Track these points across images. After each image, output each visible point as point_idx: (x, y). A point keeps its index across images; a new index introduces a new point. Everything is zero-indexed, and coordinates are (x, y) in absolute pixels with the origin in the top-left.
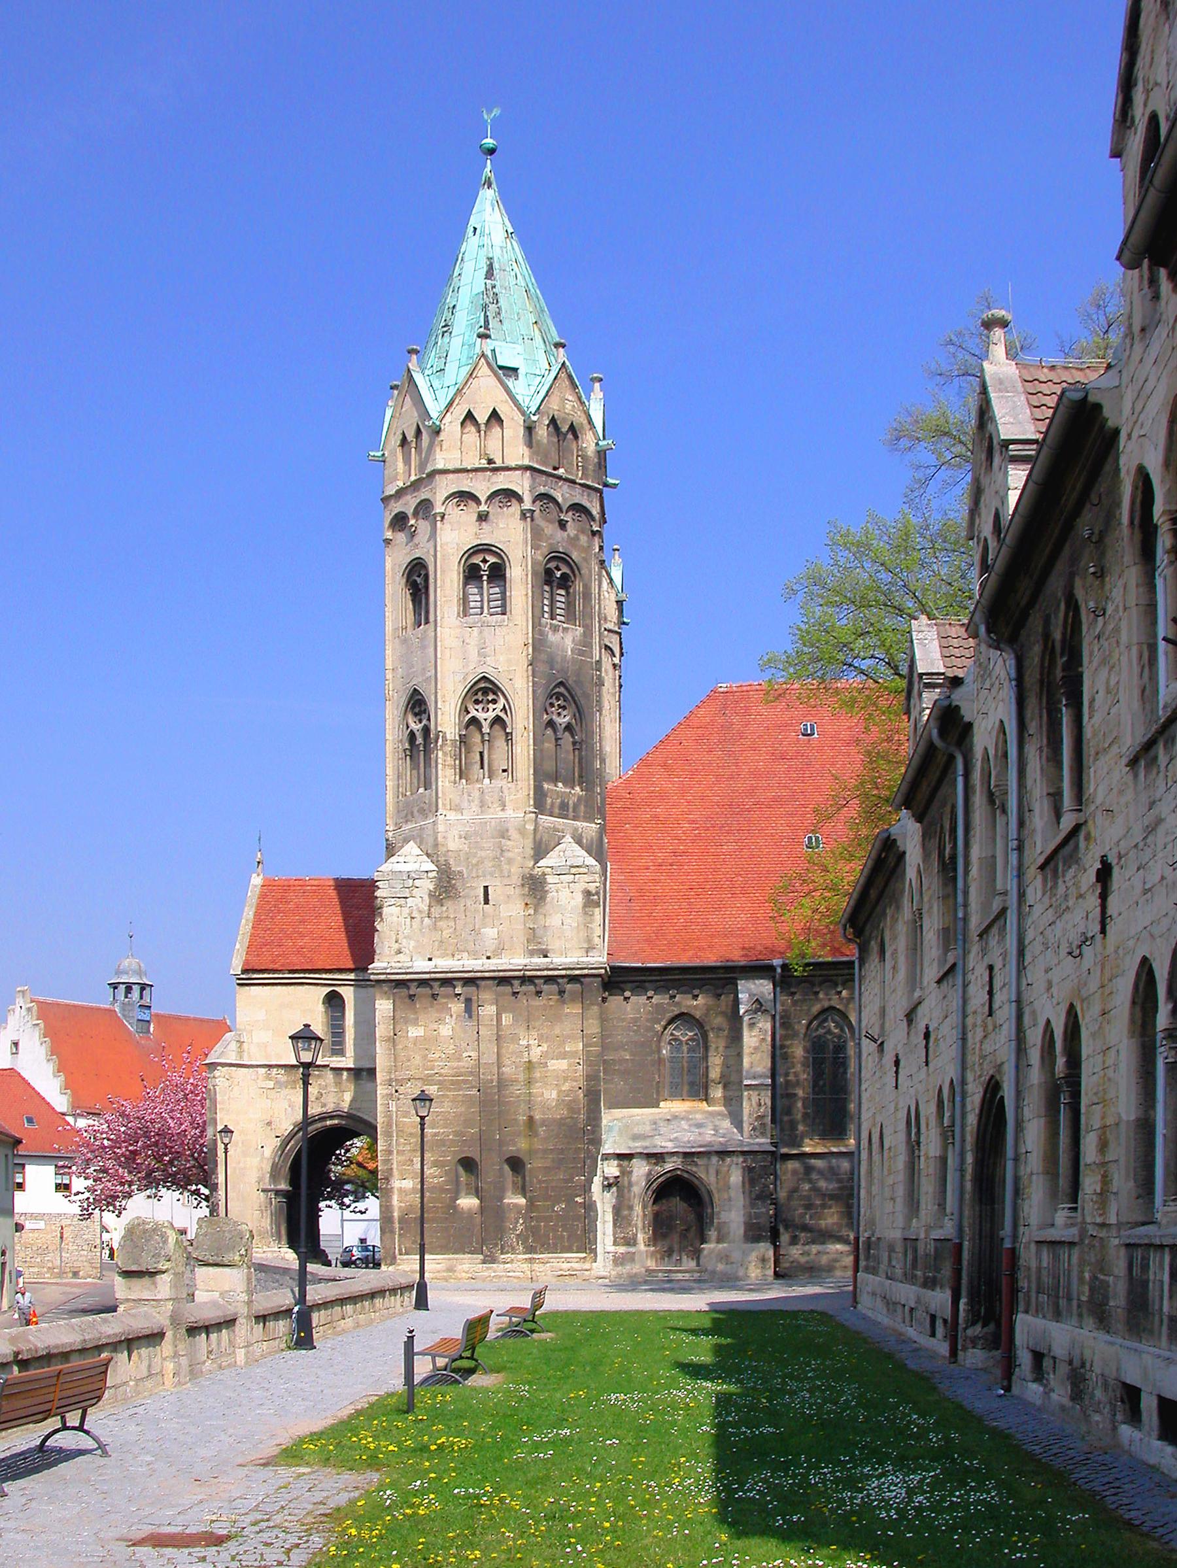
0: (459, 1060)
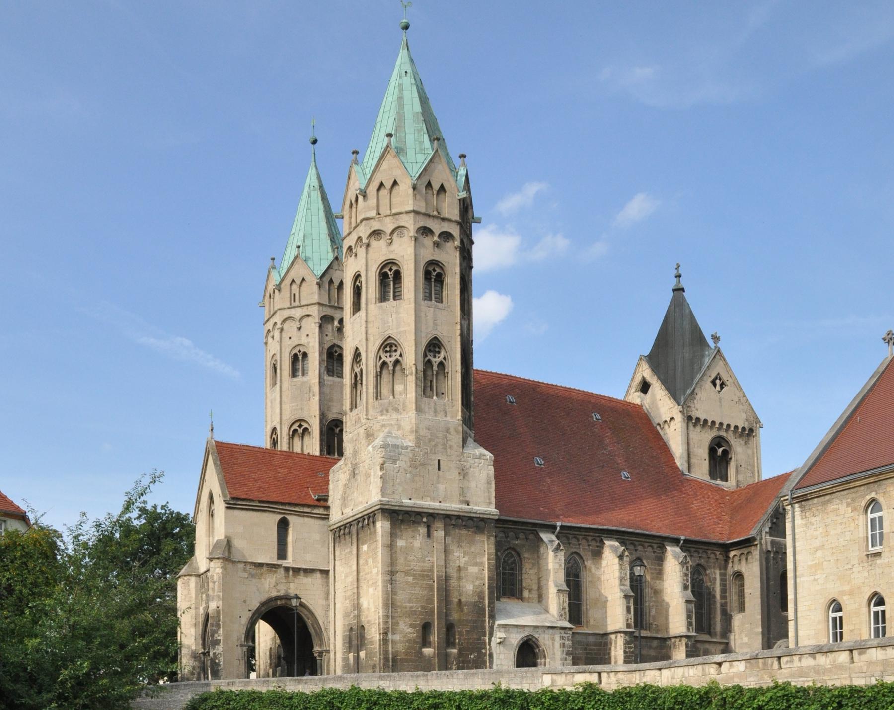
0: (424, 562)
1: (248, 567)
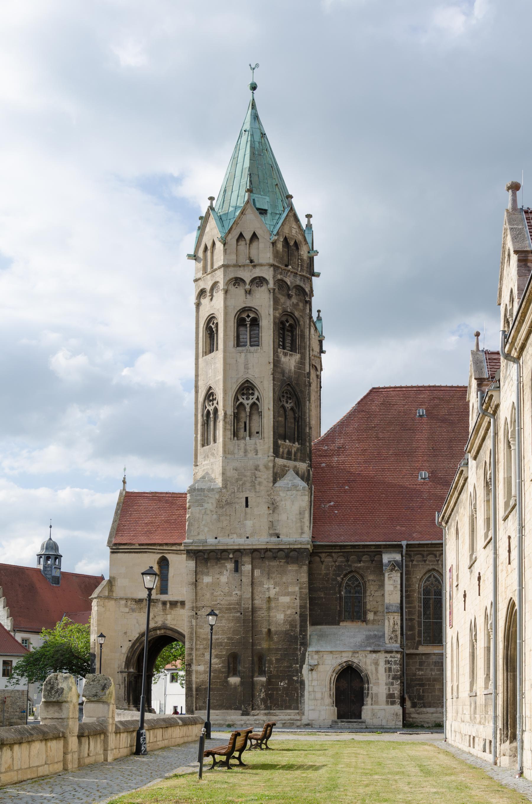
0: (231, 596)
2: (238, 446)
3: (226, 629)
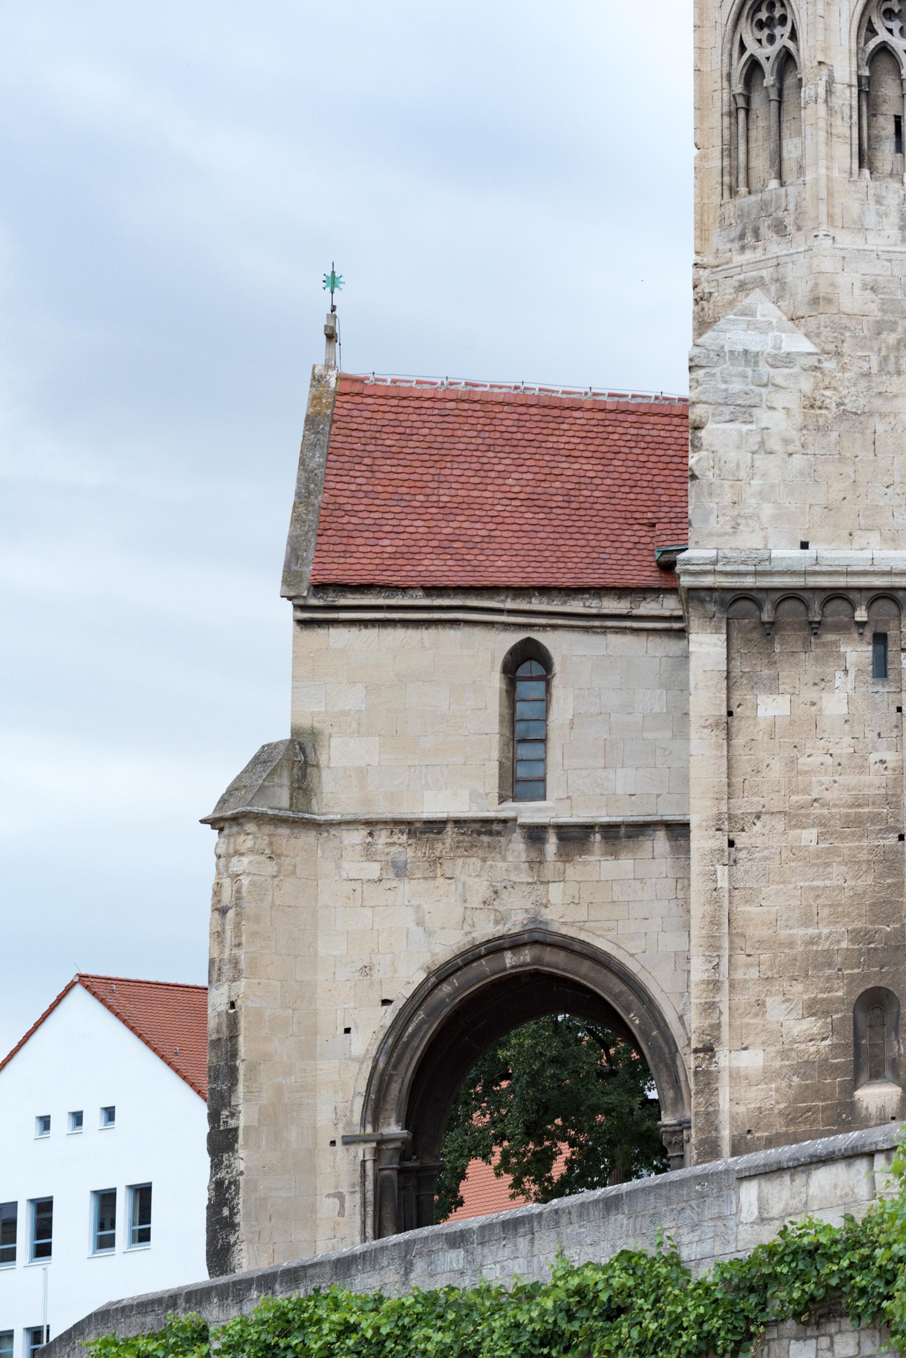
0: (862, 769)
1: (382, 837)
2: (879, 202)
3: (844, 898)
